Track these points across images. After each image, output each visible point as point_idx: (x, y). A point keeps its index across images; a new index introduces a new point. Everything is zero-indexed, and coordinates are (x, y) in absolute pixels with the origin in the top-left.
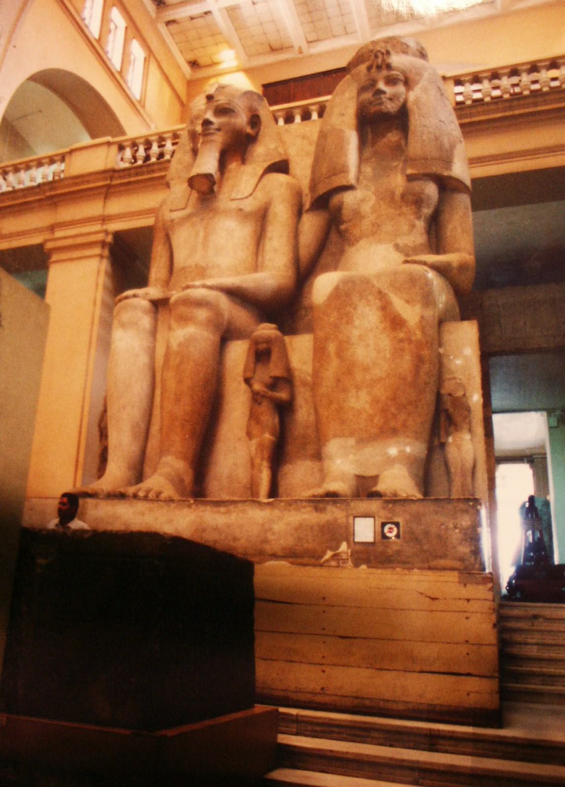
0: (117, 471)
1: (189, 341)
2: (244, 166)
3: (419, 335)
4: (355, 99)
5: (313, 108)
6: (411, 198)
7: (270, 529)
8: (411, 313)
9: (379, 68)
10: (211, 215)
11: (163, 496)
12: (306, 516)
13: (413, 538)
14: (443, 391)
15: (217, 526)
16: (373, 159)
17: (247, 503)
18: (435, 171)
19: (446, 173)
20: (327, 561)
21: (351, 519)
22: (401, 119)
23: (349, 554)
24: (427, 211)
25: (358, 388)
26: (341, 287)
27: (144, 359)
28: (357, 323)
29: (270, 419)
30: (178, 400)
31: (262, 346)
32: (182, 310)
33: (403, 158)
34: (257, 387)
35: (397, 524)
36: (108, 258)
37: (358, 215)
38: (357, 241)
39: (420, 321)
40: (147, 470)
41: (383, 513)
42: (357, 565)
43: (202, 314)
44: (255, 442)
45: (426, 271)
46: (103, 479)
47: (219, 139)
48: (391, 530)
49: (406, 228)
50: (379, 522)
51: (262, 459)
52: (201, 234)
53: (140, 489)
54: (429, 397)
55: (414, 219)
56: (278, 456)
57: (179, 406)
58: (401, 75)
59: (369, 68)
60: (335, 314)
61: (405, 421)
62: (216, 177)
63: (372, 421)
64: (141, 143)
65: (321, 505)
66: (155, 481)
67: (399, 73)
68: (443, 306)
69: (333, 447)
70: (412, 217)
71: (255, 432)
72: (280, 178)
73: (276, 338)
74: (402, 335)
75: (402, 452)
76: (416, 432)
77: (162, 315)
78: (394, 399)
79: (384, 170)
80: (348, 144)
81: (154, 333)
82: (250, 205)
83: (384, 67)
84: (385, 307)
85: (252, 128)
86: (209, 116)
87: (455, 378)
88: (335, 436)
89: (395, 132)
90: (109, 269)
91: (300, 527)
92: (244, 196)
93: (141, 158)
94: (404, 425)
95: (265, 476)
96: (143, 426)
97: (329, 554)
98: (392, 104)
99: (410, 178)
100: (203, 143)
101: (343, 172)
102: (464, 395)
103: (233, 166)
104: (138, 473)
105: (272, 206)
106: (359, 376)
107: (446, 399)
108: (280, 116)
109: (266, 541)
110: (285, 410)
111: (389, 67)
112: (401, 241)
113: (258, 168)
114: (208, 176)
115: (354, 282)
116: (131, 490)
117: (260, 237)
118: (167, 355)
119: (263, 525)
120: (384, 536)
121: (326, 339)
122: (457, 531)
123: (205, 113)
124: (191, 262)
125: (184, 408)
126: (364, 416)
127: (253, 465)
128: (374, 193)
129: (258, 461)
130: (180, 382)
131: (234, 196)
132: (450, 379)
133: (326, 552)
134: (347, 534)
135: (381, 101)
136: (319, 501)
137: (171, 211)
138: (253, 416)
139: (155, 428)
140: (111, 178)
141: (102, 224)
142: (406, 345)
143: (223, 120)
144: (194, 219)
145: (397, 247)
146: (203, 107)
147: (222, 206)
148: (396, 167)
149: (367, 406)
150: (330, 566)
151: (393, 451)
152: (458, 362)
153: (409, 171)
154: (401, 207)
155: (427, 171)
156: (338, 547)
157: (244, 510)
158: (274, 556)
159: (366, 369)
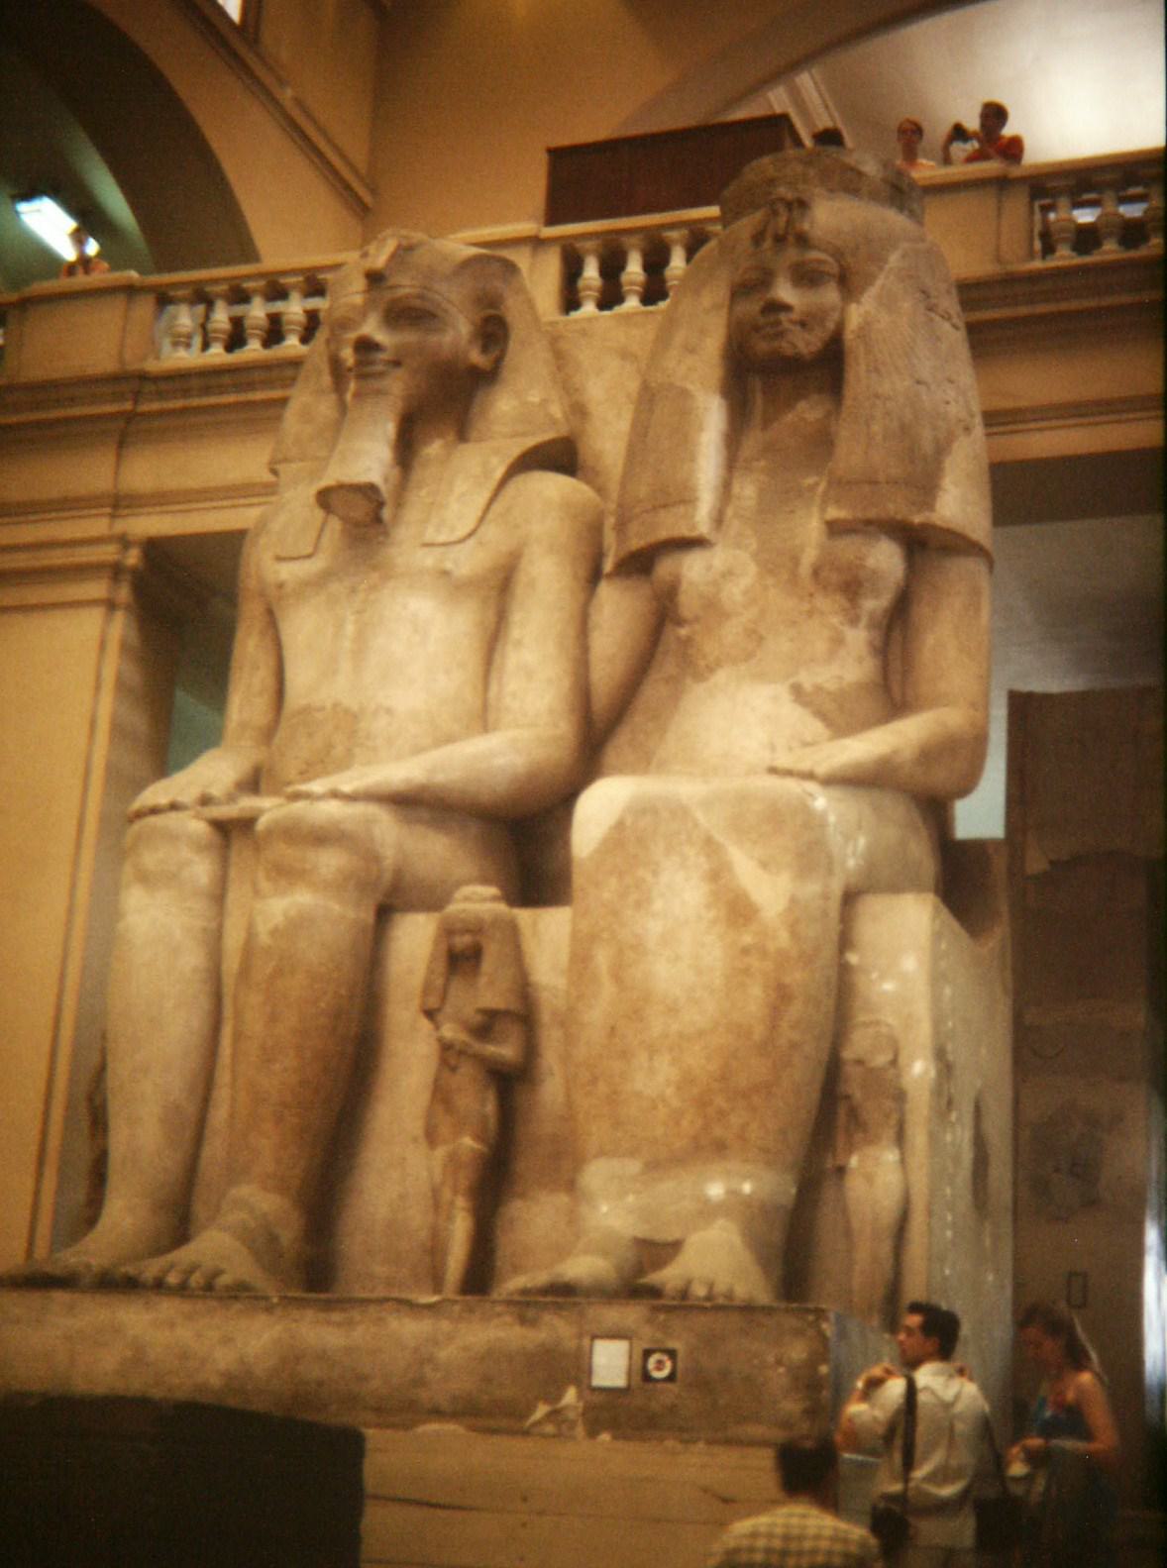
0: (125, 1214)
1: (298, 924)
2: (463, 447)
3: (783, 939)
4: (724, 312)
5: (674, 235)
6: (834, 577)
7: (431, 1359)
8: (771, 891)
9: (780, 240)
10: (375, 576)
11: (224, 1280)
12: (502, 1334)
13: (701, 1383)
14: (847, 1054)
15: (324, 1351)
16: (762, 463)
17: (387, 1305)
18: (892, 513)
19: (917, 519)
20: (538, 1423)
21: (586, 1341)
22: (829, 367)
23: (580, 1410)
24: (875, 604)
25: (652, 1051)
26: (629, 822)
27: (193, 959)
28: (658, 905)
29: (477, 1102)
30: (268, 1056)
31: (462, 941)
32: (282, 851)
33: (826, 472)
34: (449, 1031)
35: (672, 1354)
36: (128, 608)
37: (713, 608)
38: (711, 670)
39: (789, 910)
40: (200, 1210)
41: (647, 1332)
42: (592, 1433)
43: (330, 862)
44: (441, 1152)
45: (811, 795)
46: (93, 1235)
47: (397, 386)
48: (660, 1365)
49: (821, 646)
50: (641, 1346)
51: (455, 1192)
52: (350, 628)
53: (172, 1266)
54: (804, 1074)
55: (842, 624)
56: (494, 1180)
57: (267, 1071)
58: (830, 259)
59: (758, 238)
60: (613, 882)
61: (744, 1127)
62: (385, 490)
63: (677, 1123)
64: (218, 296)
65: (530, 1313)
66: (215, 1246)
67: (822, 256)
68: (862, 863)
69: (596, 1175)
70: (835, 620)
71: (444, 1130)
72: (551, 485)
73: (497, 921)
74: (747, 939)
75: (732, 1193)
76: (765, 1150)
77: (240, 852)
78: (724, 1077)
79: (779, 500)
80: (701, 429)
81: (218, 896)
82: (468, 561)
83: (791, 239)
84: (718, 873)
85: (485, 349)
86: (372, 328)
87: (878, 1023)
88: (602, 1153)
89: (815, 397)
90: (134, 638)
91: (490, 1355)
92: (453, 538)
93: (221, 336)
94: (742, 1137)
95: (460, 1230)
96: (191, 1109)
97: (542, 1410)
98: (807, 336)
99: (835, 529)
100: (357, 395)
101: (683, 502)
102: (894, 1062)
103: (434, 449)
104: (178, 1219)
105: (524, 563)
106: (657, 1026)
107: (852, 1072)
108: (588, 252)
109: (420, 1382)
110: (510, 1084)
111: (803, 241)
112: (807, 679)
113: (495, 460)
114: (369, 490)
115: (655, 812)
116: (151, 1269)
117: (493, 639)
118: (249, 949)
119: (416, 1350)
120: (647, 1377)
121: (593, 938)
122: (781, 1370)
123: (364, 314)
124: (325, 696)
125: (280, 1077)
126: (662, 1112)
127: (436, 1206)
128: (755, 556)
129: (447, 1194)
130: (273, 1018)
131: (430, 534)
132: (866, 1025)
133: (535, 1407)
134: (578, 1369)
135: (780, 328)
136: (528, 1304)
137: (280, 559)
138: (441, 1095)
139: (219, 1115)
140: (137, 396)
141: (113, 516)
142: (754, 962)
143: (410, 337)
144: (335, 587)
145: (797, 692)
146: (358, 300)
147: (399, 560)
148: (812, 488)
149: (669, 1091)
150: (544, 1436)
151: (716, 1190)
152: (888, 986)
153: (833, 513)
154: (811, 595)
155: (872, 513)
156: (559, 1397)
157: (380, 1319)
158: (437, 1413)
159: (673, 1010)
